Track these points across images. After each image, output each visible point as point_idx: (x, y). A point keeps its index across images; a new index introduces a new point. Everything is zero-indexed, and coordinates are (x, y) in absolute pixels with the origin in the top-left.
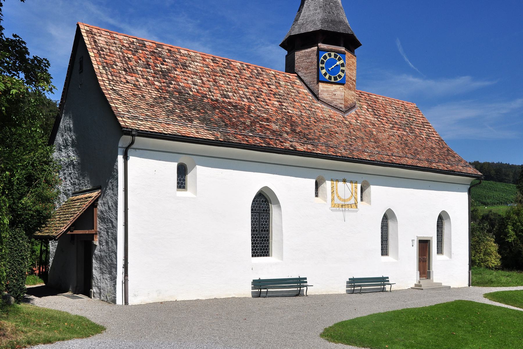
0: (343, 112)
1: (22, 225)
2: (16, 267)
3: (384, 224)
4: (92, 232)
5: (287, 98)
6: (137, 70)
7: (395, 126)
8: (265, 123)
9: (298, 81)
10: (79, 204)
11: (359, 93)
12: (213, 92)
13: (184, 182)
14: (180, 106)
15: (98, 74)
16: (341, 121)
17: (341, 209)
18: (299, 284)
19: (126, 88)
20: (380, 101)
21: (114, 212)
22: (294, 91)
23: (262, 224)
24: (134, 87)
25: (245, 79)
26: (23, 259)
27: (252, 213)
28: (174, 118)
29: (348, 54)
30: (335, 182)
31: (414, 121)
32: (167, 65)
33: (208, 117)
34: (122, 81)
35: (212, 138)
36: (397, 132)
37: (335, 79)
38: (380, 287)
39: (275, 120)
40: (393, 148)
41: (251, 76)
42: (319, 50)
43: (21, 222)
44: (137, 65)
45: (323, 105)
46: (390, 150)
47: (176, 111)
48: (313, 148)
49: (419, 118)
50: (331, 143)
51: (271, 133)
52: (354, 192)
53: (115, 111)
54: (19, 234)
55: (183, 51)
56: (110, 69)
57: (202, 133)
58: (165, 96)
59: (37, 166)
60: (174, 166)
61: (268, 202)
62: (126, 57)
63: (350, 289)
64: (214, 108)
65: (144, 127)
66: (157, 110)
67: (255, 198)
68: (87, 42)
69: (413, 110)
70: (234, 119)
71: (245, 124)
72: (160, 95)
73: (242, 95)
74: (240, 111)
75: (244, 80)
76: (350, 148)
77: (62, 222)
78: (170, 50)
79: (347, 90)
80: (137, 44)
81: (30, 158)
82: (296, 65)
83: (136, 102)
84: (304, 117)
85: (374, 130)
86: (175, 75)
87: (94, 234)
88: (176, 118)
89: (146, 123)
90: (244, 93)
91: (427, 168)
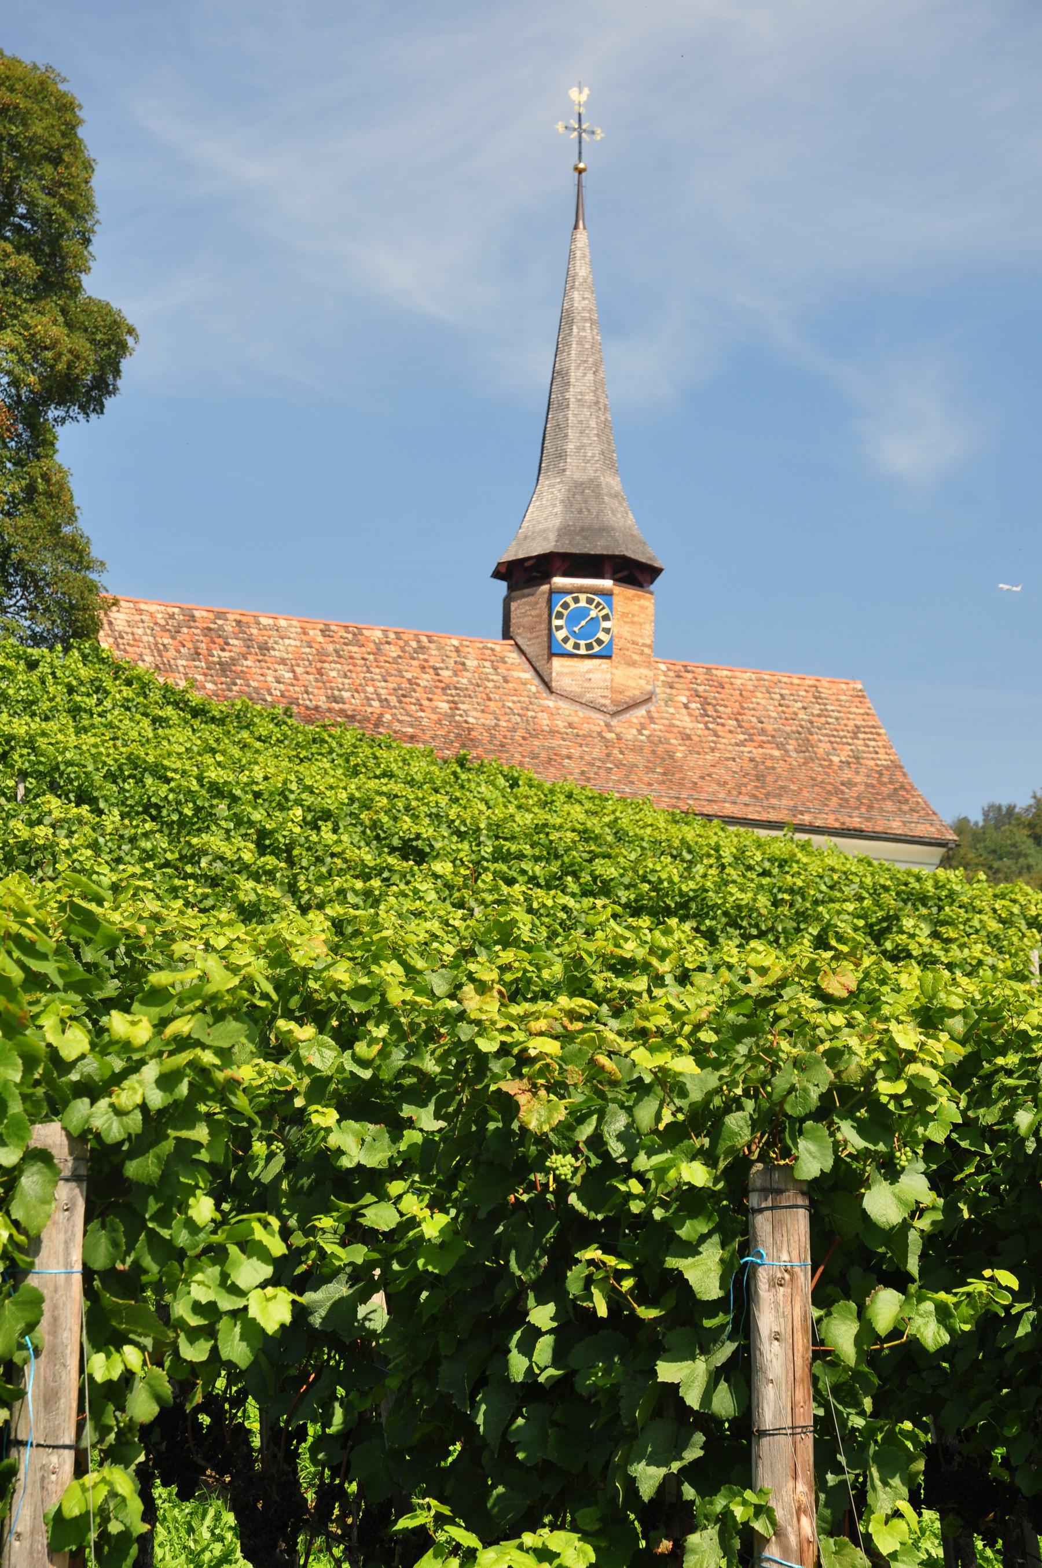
9: (513, 657)
22: (495, 678)
55: (264, 621)
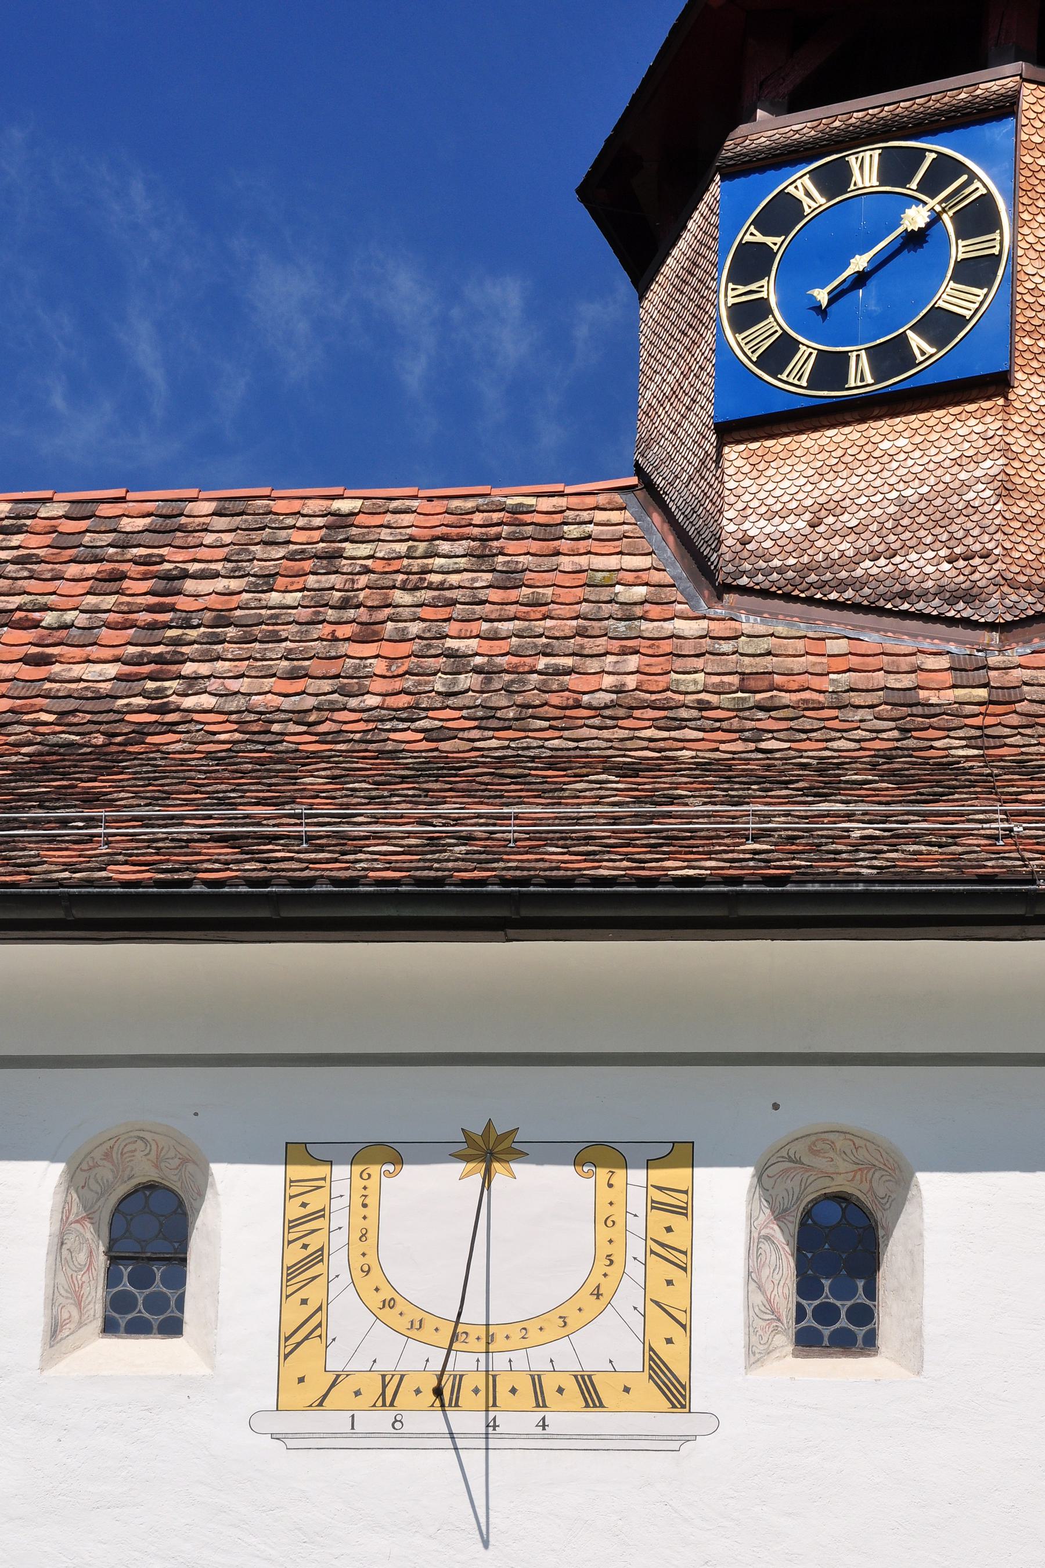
30: (341, 1171)
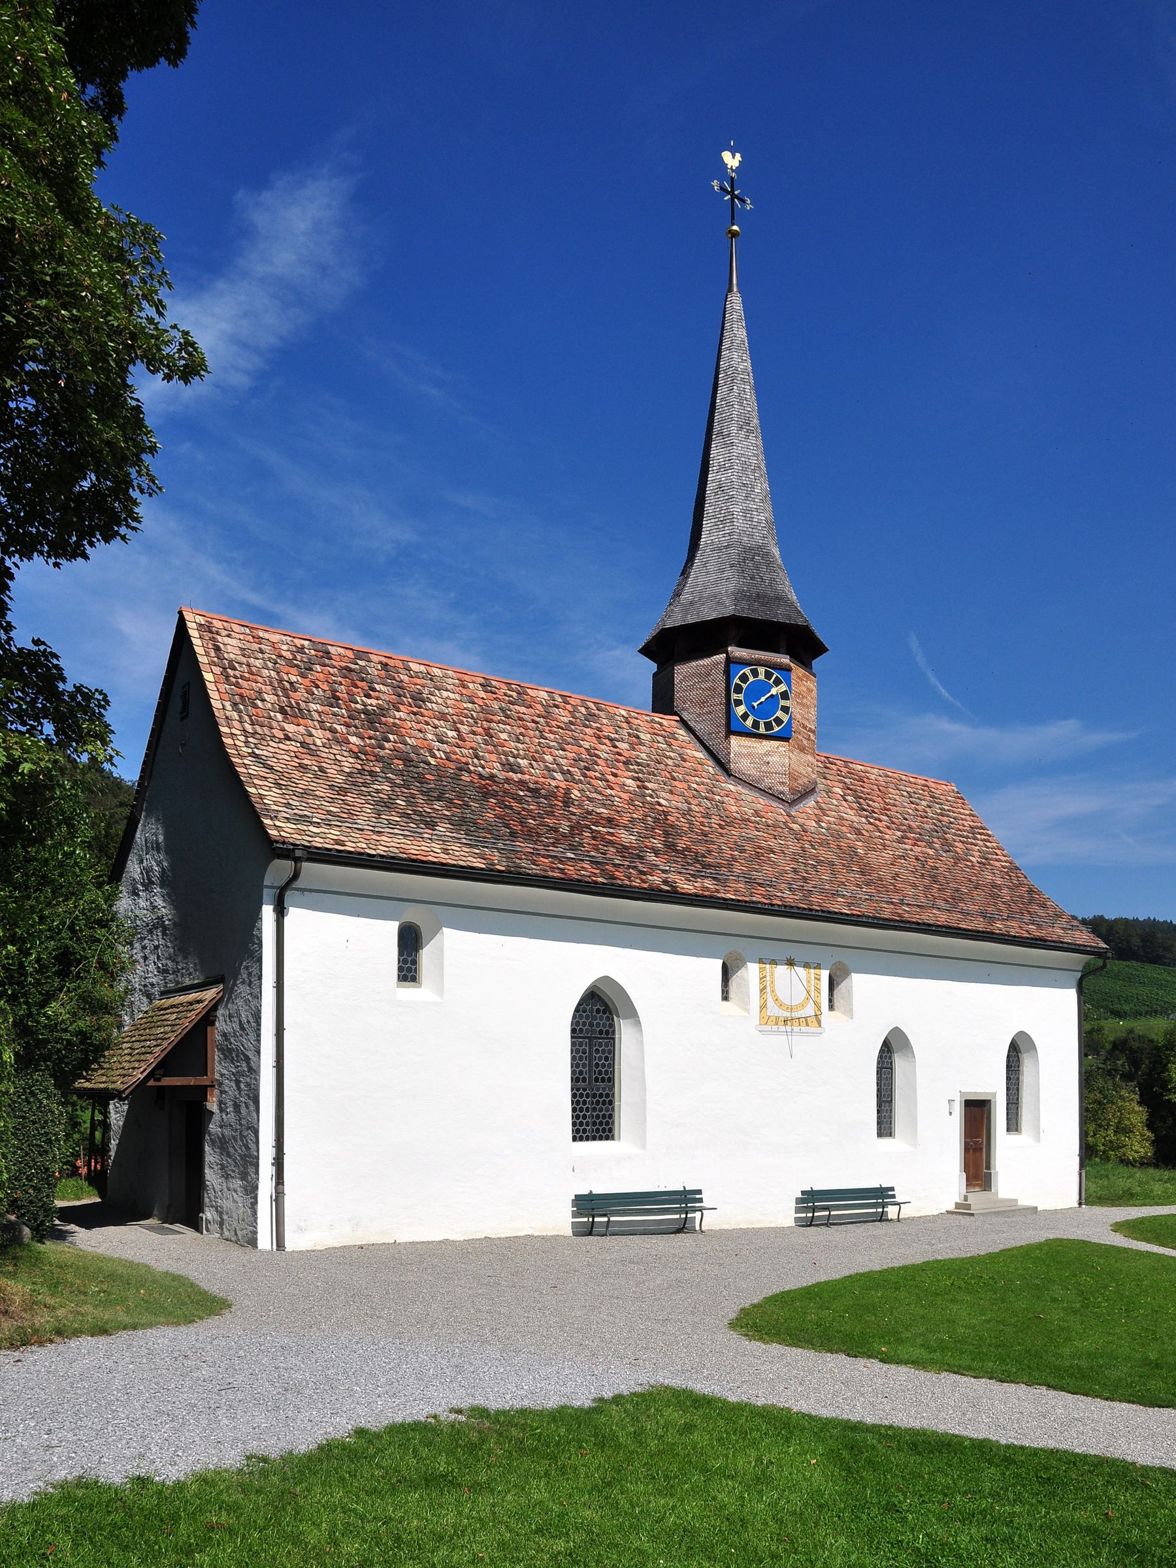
0: (788, 802)
1: (47, 1066)
2: (33, 1160)
3: (883, 1062)
4: (203, 1081)
5: (656, 772)
6: (309, 711)
7: (909, 835)
8: (605, 830)
10: (174, 1016)
11: (823, 758)
12: (483, 758)
13: (413, 967)
14: (406, 791)
15: (221, 721)
16: (781, 825)
17: (782, 1028)
18: (684, 1205)
19: (283, 752)
20: (873, 777)
21: (252, 1037)
22: (672, 754)
23: (597, 1065)
24: (301, 750)
25: (559, 727)
26: (49, 1142)
27: (572, 1037)
28: (391, 818)
29: (798, 671)
30: (768, 966)
31: (951, 823)
32: (377, 698)
33: (472, 816)
34: (274, 736)
35: (479, 864)
36: (912, 850)
37: (768, 726)
38: (874, 1210)
39: (629, 821)
40: (904, 886)
41: (573, 720)
42: (729, 661)
43: (46, 1058)
44: (311, 700)
45: (740, 788)
46: (896, 891)
47: (398, 801)
48: (717, 887)
49: (963, 817)
50: (760, 874)
51: (618, 851)
52: (813, 988)
53: (256, 805)
54: (41, 1085)
55: (414, 667)
56: (250, 708)
57: (457, 853)
58: (373, 769)
59: (81, 931)
60: (391, 929)
61: (611, 1013)
62: (284, 682)
63: (804, 1215)
64: (486, 794)
65: (321, 840)
66: (353, 800)
67: (579, 1004)
68: (199, 650)
69: (950, 798)
70: (531, 821)
71: (556, 830)
72: (360, 767)
73: (551, 766)
74: (546, 802)
75: (556, 730)
76: (803, 886)
77: (137, 1057)
78: (387, 665)
79: (796, 752)
80: (312, 651)
81: (66, 912)
82: (677, 695)
83: (306, 783)
84: (697, 814)
85: (860, 844)
86: (397, 721)
87: (207, 1086)
88: (398, 819)
89: (327, 831)
90: (554, 759)
91: (983, 932)
